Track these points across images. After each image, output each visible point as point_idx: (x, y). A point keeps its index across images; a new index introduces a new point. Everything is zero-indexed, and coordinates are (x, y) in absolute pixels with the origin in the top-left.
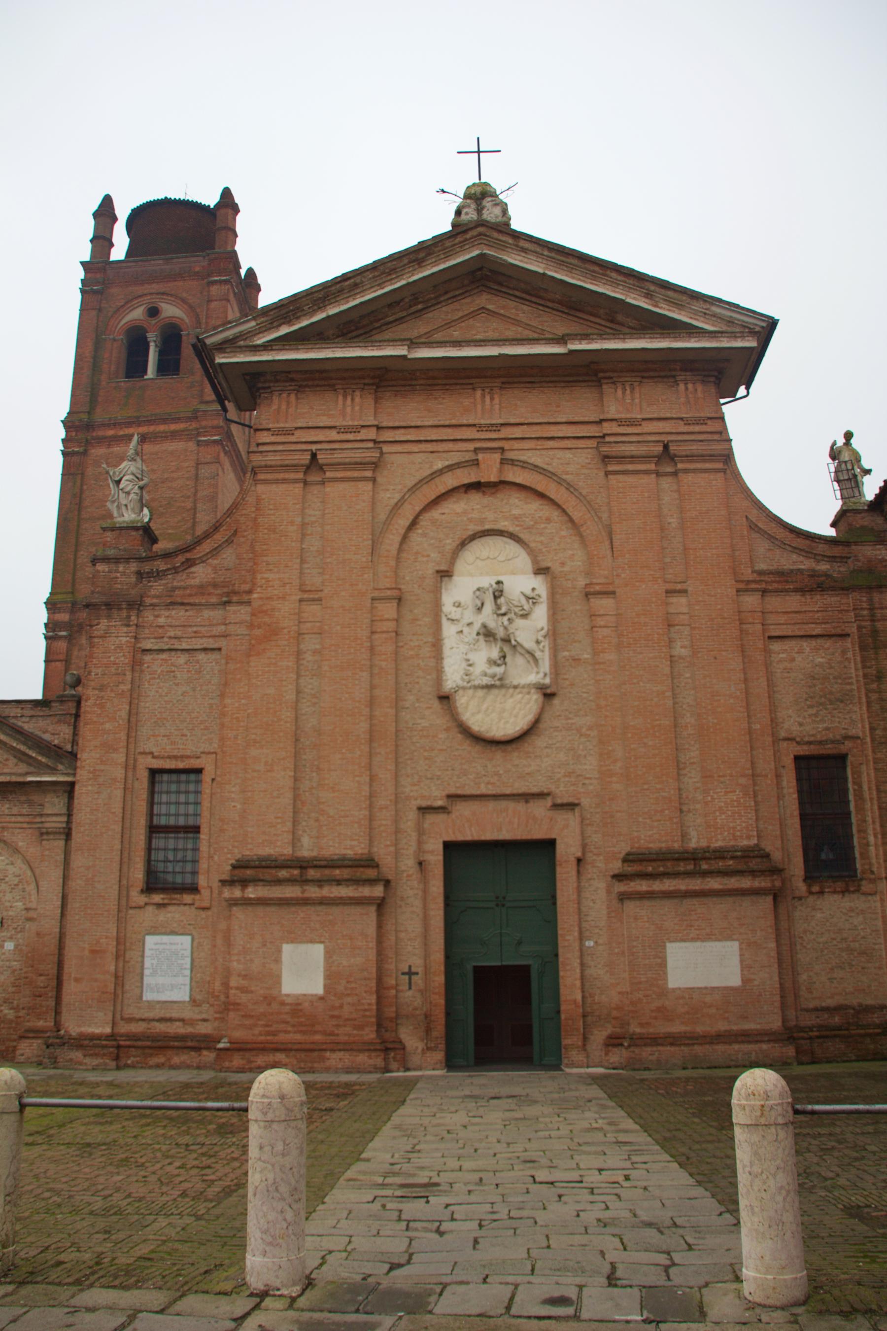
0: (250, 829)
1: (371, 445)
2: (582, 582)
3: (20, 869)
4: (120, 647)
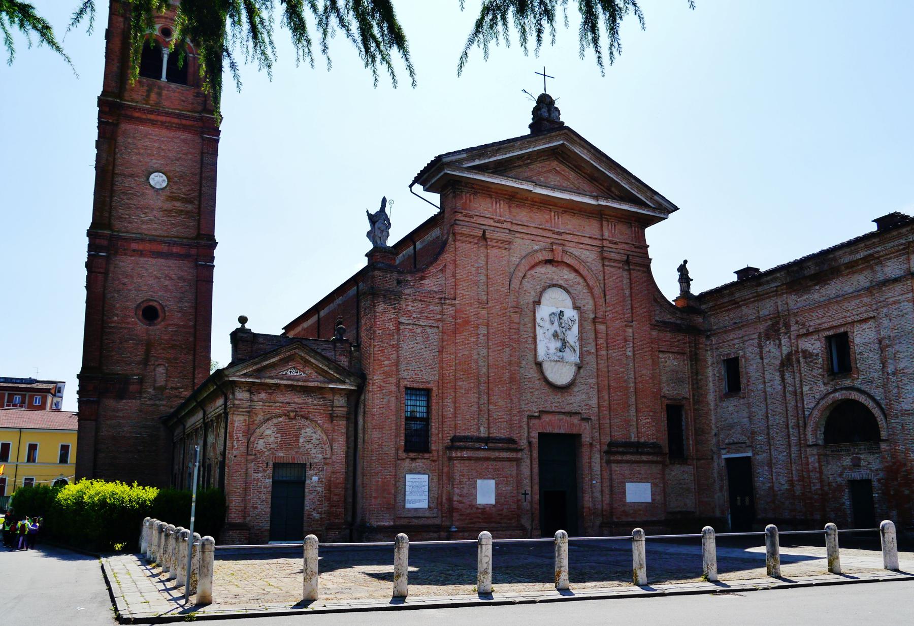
0: (459, 422)
1: (507, 231)
2: (592, 316)
3: (320, 436)
4: (390, 320)
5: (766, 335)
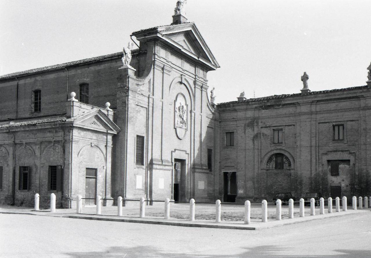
5: (248, 125)
